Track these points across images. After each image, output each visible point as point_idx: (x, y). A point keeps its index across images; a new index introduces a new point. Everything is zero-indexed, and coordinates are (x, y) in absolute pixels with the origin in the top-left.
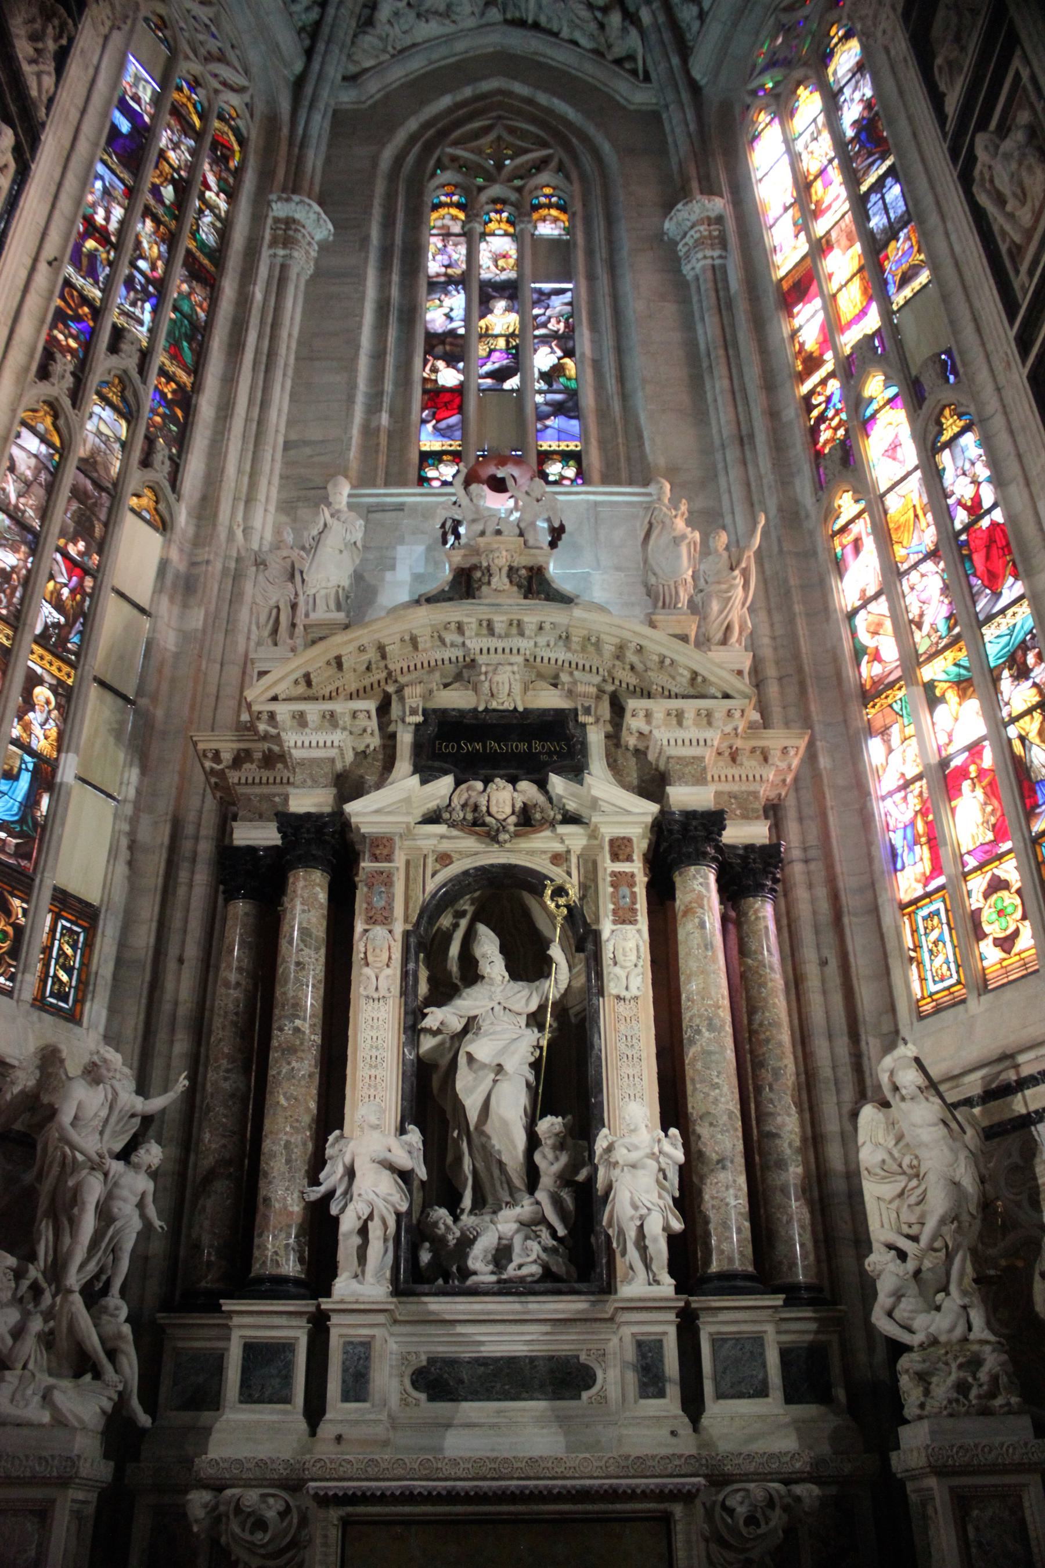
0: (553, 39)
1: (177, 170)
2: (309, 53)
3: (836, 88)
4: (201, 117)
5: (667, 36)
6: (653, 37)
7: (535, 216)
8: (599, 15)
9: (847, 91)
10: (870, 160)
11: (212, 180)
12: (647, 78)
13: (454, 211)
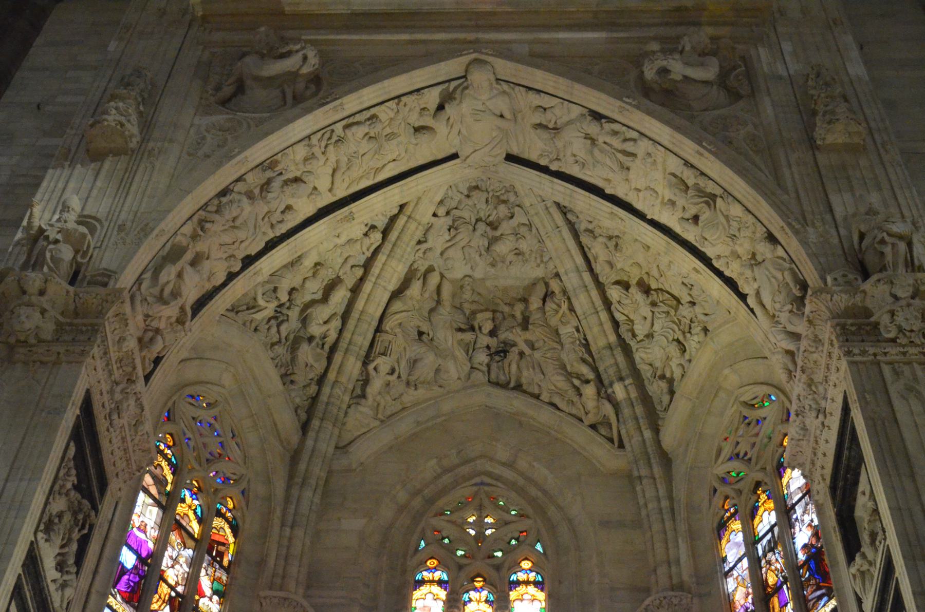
0: (534, 401)
1: (172, 588)
2: (305, 427)
3: (789, 503)
4: (200, 521)
5: (639, 410)
6: (626, 411)
7: (513, 595)
8: (577, 382)
9: (799, 510)
10: (819, 593)
11: (206, 583)
12: (621, 446)
13: (436, 589)
